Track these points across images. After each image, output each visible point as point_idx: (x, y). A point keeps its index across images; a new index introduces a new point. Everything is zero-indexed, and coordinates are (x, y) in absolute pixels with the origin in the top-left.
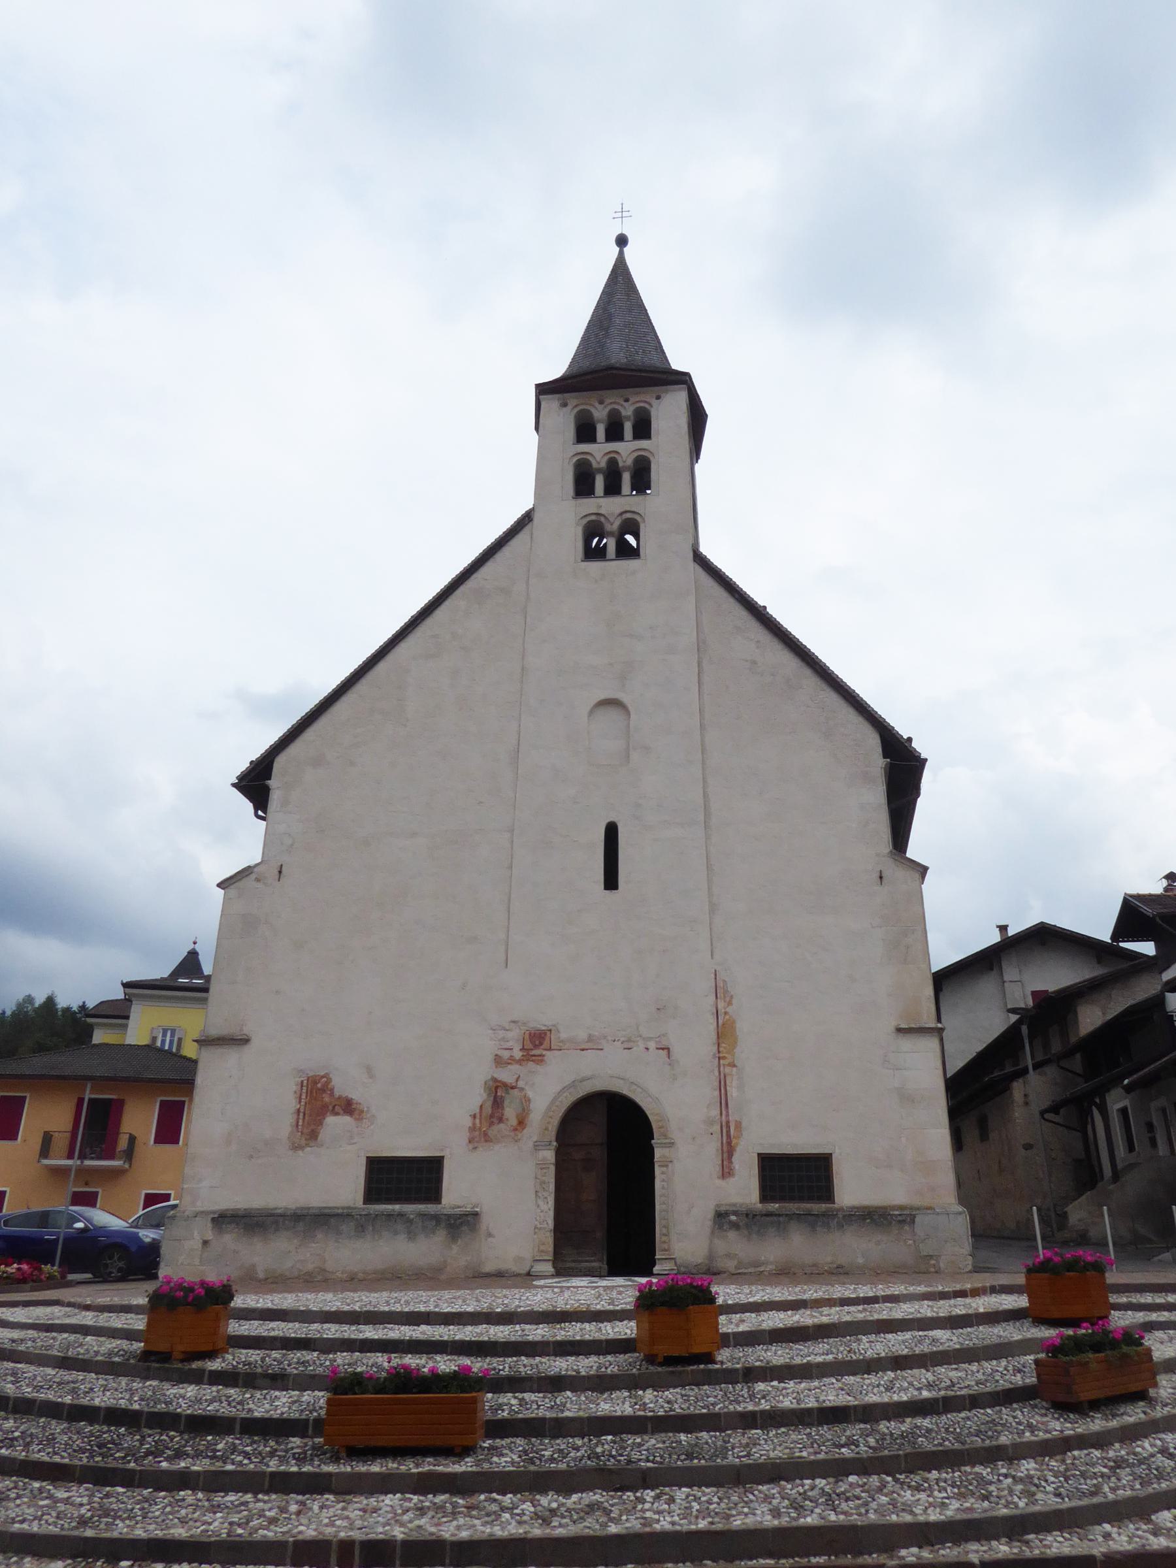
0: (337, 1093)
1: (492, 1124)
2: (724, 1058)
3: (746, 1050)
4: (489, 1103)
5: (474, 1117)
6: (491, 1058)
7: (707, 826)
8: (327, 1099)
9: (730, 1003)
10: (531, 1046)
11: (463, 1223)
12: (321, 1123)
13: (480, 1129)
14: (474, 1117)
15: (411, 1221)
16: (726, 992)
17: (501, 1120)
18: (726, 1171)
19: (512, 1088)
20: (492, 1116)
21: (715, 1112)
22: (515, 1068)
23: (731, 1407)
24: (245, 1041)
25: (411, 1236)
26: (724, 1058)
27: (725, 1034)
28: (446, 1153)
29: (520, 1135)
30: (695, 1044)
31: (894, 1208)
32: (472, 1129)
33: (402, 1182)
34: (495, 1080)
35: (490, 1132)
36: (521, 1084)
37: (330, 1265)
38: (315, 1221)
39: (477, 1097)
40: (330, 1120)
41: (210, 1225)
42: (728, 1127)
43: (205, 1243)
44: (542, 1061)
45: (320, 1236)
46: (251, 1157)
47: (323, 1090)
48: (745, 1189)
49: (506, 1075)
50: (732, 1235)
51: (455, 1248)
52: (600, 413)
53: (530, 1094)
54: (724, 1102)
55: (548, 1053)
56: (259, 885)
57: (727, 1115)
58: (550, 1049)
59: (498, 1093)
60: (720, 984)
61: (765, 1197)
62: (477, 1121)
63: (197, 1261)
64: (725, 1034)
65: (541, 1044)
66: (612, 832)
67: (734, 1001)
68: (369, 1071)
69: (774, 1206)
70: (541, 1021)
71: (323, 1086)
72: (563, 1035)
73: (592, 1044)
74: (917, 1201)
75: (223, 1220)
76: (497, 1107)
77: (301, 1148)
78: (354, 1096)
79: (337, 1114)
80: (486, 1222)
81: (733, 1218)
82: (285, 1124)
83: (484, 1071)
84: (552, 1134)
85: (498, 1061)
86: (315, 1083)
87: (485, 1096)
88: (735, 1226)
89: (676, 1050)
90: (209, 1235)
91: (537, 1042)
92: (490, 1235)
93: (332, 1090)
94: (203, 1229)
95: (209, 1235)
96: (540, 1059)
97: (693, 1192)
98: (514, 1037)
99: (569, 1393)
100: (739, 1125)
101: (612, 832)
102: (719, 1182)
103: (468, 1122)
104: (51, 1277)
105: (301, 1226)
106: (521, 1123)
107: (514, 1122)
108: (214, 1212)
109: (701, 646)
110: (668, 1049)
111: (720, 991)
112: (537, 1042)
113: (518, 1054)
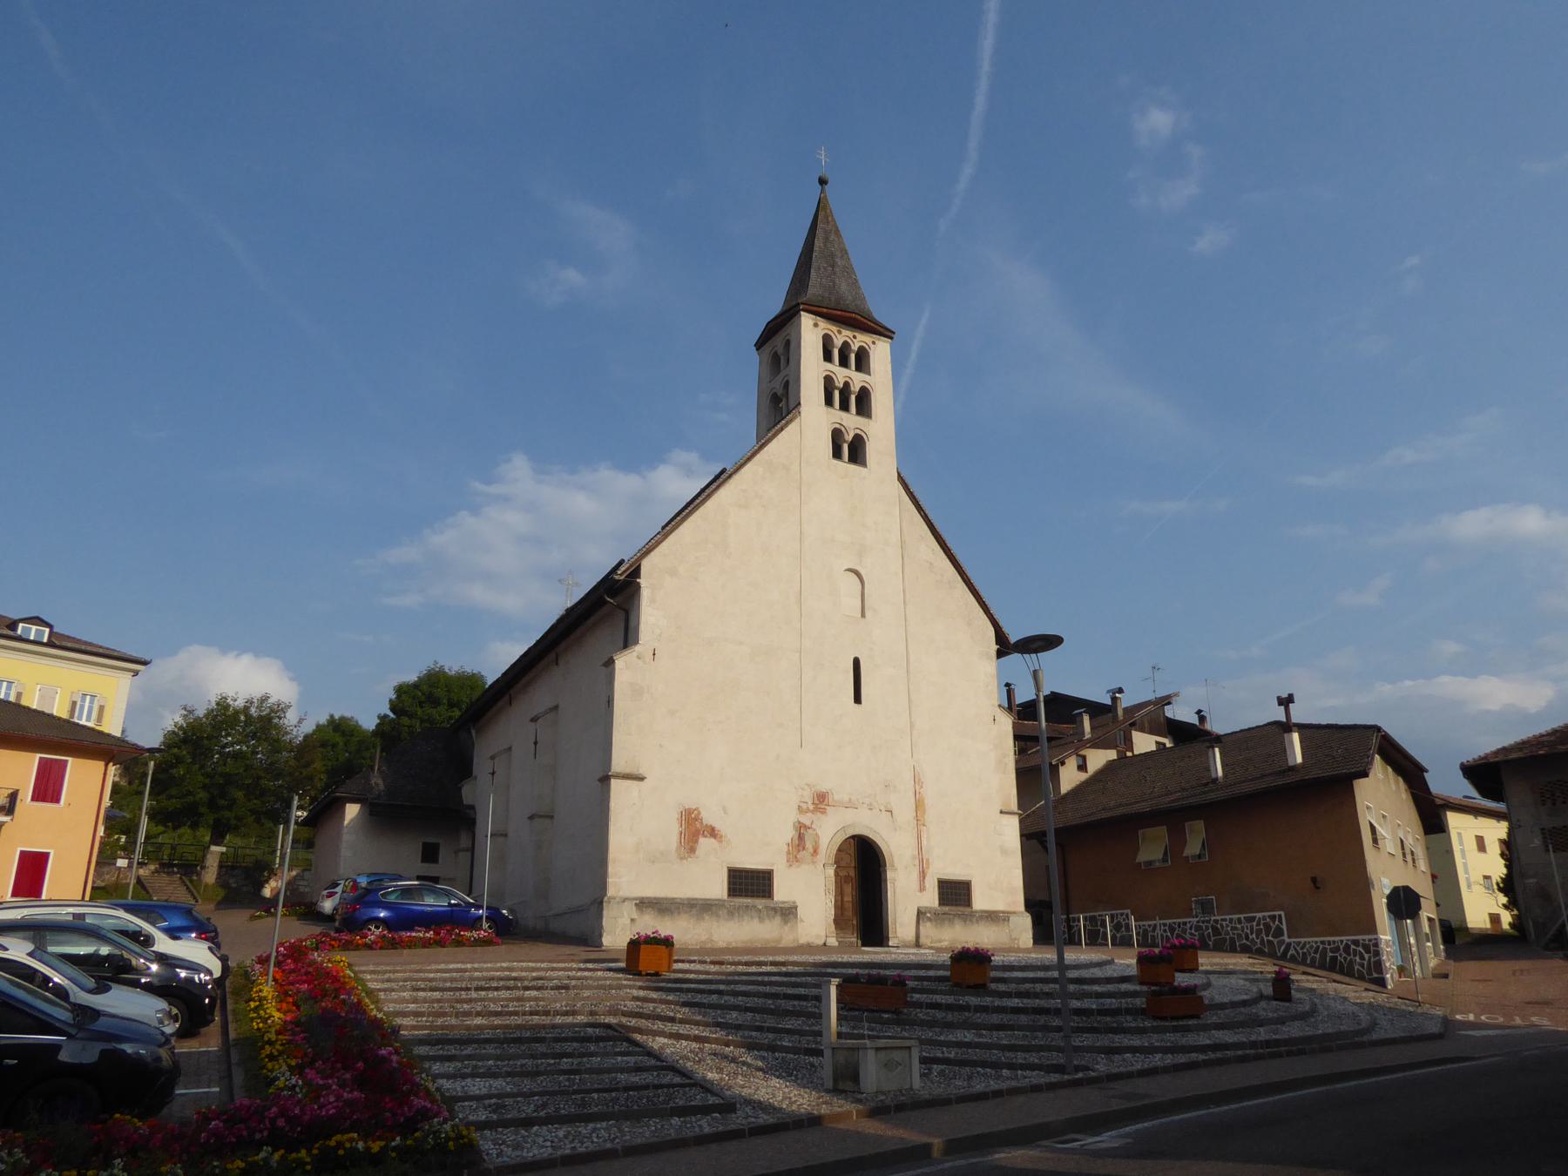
3: (930, 816)
11: (788, 913)
18: (922, 889)
24: (641, 779)
25: (761, 920)
27: (919, 805)
30: (905, 813)
33: (750, 885)
37: (715, 938)
38: (701, 908)
39: (789, 834)
40: (702, 840)
43: (633, 920)
47: (696, 819)
48: (931, 899)
49: (806, 820)
52: (838, 341)
54: (920, 849)
59: (801, 831)
64: (919, 805)
66: (856, 663)
69: (946, 909)
70: (823, 788)
73: (851, 805)
75: (644, 904)
76: (801, 840)
78: (717, 825)
82: (673, 839)
83: (793, 816)
84: (832, 860)
88: (930, 919)
94: (629, 911)
95: (635, 916)
96: (824, 812)
97: (907, 898)
98: (808, 796)
101: (856, 663)
103: (785, 848)
106: (815, 852)
111: (917, 780)
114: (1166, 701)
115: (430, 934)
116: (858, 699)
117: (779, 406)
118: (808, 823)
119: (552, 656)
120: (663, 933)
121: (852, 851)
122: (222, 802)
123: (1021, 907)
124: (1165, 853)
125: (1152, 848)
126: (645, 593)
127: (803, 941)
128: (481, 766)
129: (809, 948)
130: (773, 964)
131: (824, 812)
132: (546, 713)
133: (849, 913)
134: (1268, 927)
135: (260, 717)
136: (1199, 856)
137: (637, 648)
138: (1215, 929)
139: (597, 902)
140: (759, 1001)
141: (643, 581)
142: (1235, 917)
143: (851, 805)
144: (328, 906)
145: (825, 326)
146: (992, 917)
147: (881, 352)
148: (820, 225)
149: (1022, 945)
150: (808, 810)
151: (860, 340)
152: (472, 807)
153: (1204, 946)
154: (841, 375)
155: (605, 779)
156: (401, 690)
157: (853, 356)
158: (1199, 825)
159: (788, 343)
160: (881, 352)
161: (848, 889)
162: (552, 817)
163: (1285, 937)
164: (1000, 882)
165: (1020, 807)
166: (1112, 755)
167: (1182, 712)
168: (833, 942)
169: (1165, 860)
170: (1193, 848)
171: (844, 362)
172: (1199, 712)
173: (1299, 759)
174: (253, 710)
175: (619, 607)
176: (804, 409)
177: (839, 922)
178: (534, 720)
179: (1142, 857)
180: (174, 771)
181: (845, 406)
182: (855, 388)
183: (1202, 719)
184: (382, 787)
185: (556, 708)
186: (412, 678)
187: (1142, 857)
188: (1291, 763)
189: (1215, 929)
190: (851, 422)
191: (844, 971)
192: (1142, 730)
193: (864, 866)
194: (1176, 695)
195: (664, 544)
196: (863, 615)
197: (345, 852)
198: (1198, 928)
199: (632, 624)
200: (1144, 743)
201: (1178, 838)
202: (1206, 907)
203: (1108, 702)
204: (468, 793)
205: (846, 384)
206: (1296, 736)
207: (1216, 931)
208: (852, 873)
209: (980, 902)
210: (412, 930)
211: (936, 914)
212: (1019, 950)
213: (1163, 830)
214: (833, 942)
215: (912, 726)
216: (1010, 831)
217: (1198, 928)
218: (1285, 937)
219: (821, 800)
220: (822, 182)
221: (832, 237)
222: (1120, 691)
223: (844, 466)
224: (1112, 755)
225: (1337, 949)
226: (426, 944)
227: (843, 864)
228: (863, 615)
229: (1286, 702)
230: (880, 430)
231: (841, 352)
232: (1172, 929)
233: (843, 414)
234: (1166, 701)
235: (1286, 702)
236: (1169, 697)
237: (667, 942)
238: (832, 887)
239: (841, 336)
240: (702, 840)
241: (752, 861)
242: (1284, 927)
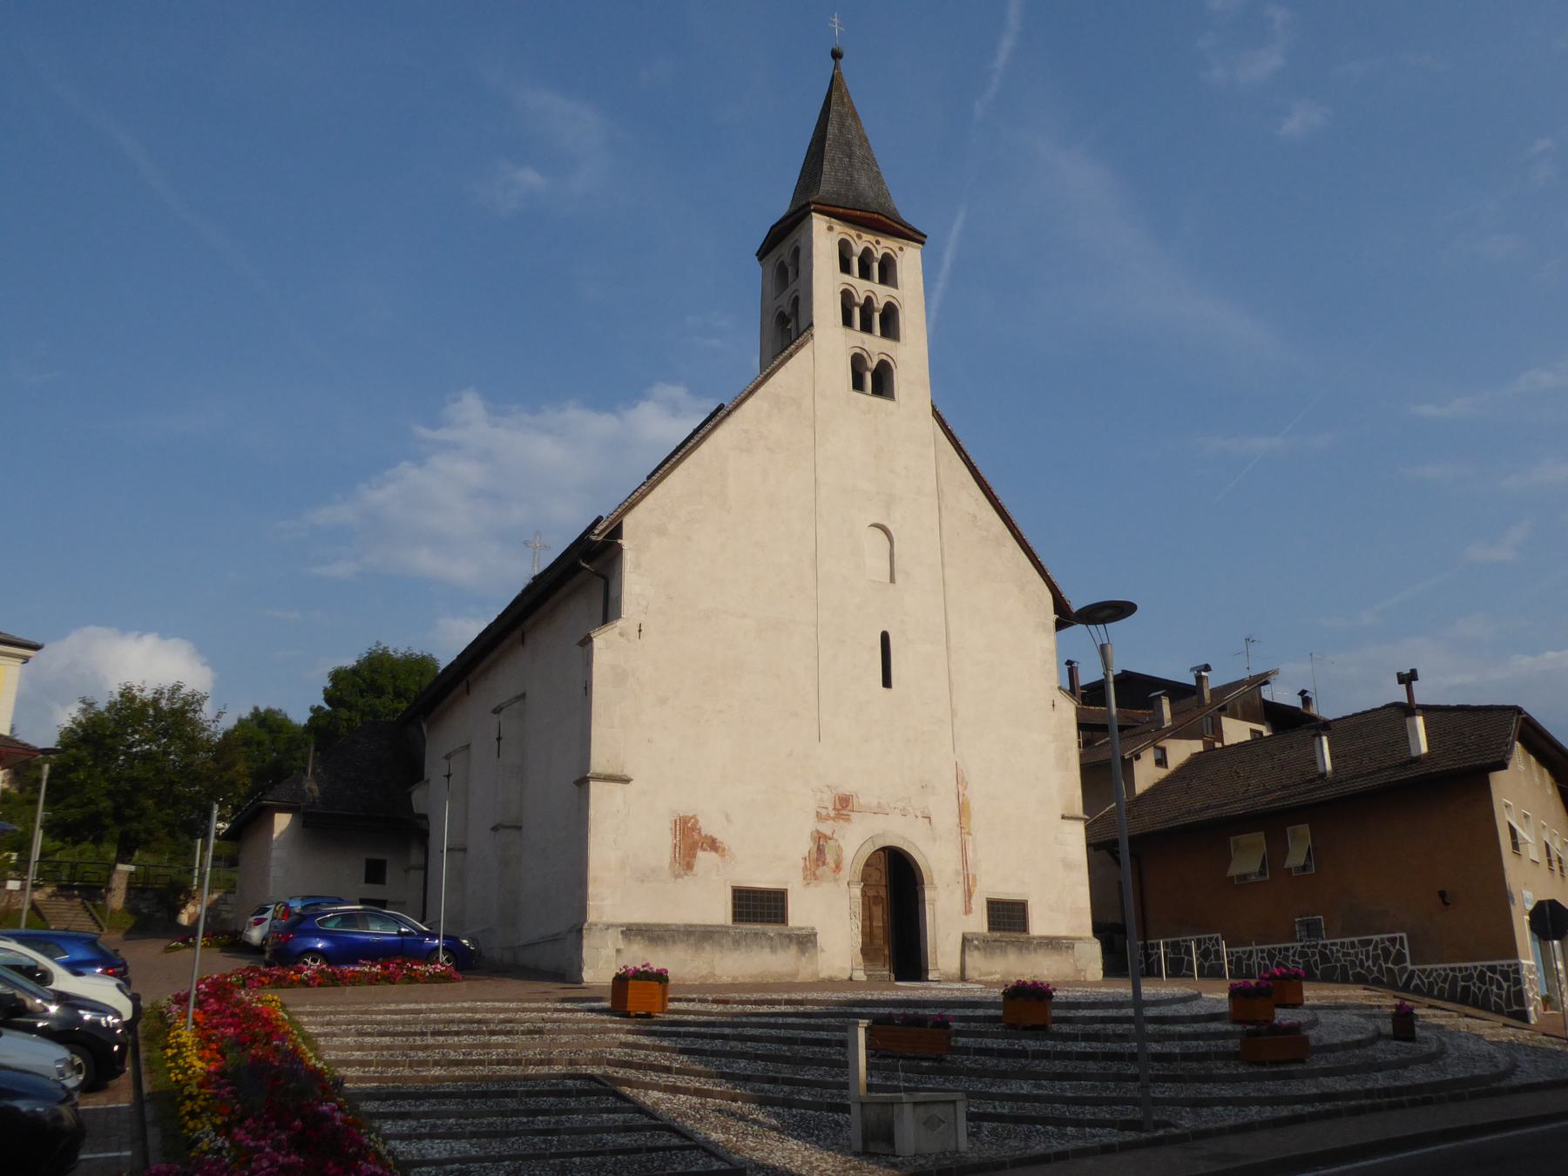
3: (977, 822)
11: (806, 941)
12: (694, 856)
15: (771, 939)
24: (626, 781)
25: (773, 949)
27: (963, 810)
28: (789, 887)
30: (947, 818)
32: (805, 869)
33: (759, 907)
37: (718, 972)
39: (805, 846)
40: (700, 854)
43: (618, 951)
48: (978, 922)
49: (826, 828)
50: (976, 954)
52: (858, 248)
54: (965, 862)
56: (622, 640)
61: (990, 929)
64: (963, 810)
66: (885, 638)
68: (727, 817)
70: (846, 789)
73: (879, 810)
75: (632, 932)
76: (820, 854)
77: (677, 877)
78: (719, 837)
80: (821, 940)
83: (809, 825)
84: (858, 877)
88: (977, 948)
94: (614, 940)
96: (847, 819)
97: (949, 922)
98: (828, 801)
101: (885, 638)
103: (802, 863)
105: (692, 940)
106: (838, 867)
111: (960, 779)
113: (832, 814)
114: (1263, 680)
115: (377, 969)
116: (887, 682)
117: (787, 328)
118: (829, 833)
119: (517, 633)
120: (656, 965)
121: (882, 866)
122: (128, 812)
123: (1087, 930)
124: (1263, 865)
125: (1246, 859)
126: (628, 557)
127: (824, 974)
128: (434, 768)
129: (831, 983)
130: (789, 1002)
131: (847, 819)
132: (510, 703)
133: (879, 941)
134: (1386, 952)
135: (173, 712)
136: (1304, 868)
137: (619, 623)
138: (1323, 956)
139: (577, 930)
140: (772, 1047)
141: (626, 542)
142: (1347, 940)
143: (879, 810)
144: (256, 935)
145: (841, 230)
146: (1053, 944)
147: (909, 260)
148: (834, 107)
149: (1090, 978)
150: (828, 818)
151: (885, 246)
152: (425, 817)
153: (1310, 976)
154: (862, 288)
155: (583, 782)
156: (338, 677)
157: (876, 266)
158: (1304, 830)
159: (797, 252)
160: (909, 260)
161: (878, 912)
162: (519, 828)
163: (1408, 964)
164: (1062, 899)
165: (1085, 811)
166: (1197, 746)
167: (1282, 693)
168: (860, 975)
169: (1262, 873)
170: (1296, 857)
171: (865, 273)
172: (1303, 693)
173: (1424, 749)
174: (163, 703)
175: (597, 574)
176: (817, 331)
177: (868, 952)
178: (497, 711)
179: (1234, 870)
180: (72, 776)
181: (866, 327)
182: (879, 304)
183: (1307, 701)
184: (317, 794)
185: (523, 696)
186: (349, 662)
187: (1234, 870)
188: (1414, 754)
189: (1323, 956)
190: (875, 346)
191: (874, 1010)
192: (1234, 716)
193: (897, 885)
194: (1275, 672)
195: (650, 497)
196: (892, 580)
197: (275, 872)
198: (1303, 955)
199: (612, 594)
200: (1236, 731)
201: (1277, 847)
202: (1312, 929)
203: (1193, 682)
204: (419, 799)
205: (869, 300)
206: (1420, 721)
207: (1325, 958)
208: (883, 893)
209: (1039, 926)
210: (356, 963)
211: (985, 941)
212: (1086, 984)
213: (1260, 837)
214: (860, 975)
215: (954, 713)
216: (1076, 836)
217: (1303, 955)
218: (1408, 964)
219: (844, 805)
220: (836, 55)
221: (849, 121)
222: (1207, 668)
223: (866, 400)
224: (1197, 746)
225: (1470, 977)
226: (373, 980)
227: (871, 881)
228: (892, 580)
229: (1408, 679)
230: (910, 355)
231: (861, 260)
232: (1271, 956)
233: (865, 336)
234: (1263, 680)
235: (1408, 679)
236: (1266, 674)
237: (661, 977)
238: (859, 910)
239: (861, 242)
240: (700, 854)
241: (761, 879)
242: (1407, 951)
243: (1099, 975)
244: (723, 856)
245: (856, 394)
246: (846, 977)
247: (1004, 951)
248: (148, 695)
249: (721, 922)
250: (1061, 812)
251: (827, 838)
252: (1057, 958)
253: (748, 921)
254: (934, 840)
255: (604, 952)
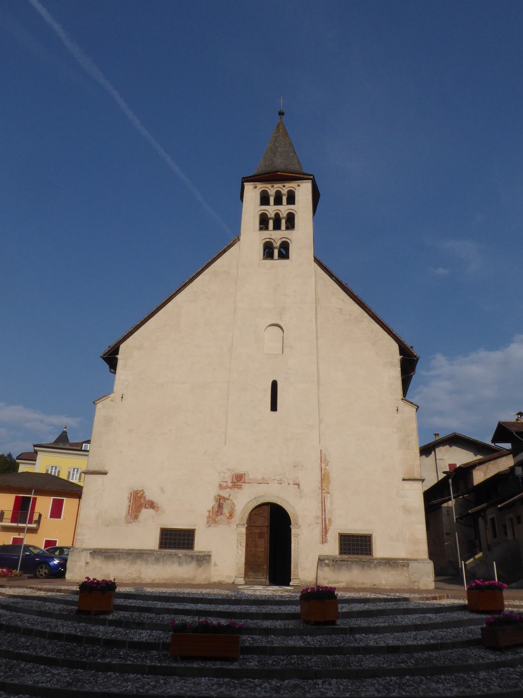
0: (147, 499)
1: (218, 515)
2: (324, 489)
3: (334, 486)
4: (217, 506)
5: (210, 511)
6: (218, 485)
7: (318, 384)
8: (142, 501)
9: (327, 465)
10: (236, 481)
11: (204, 559)
12: (140, 511)
13: (212, 517)
14: (210, 511)
15: (180, 557)
16: (326, 459)
17: (221, 514)
18: (324, 540)
19: (227, 499)
20: (218, 512)
21: (320, 514)
22: (228, 490)
23: (348, 645)
24: (106, 474)
25: (180, 564)
26: (324, 489)
27: (325, 478)
28: (196, 528)
29: (230, 521)
31: (399, 559)
32: (209, 517)
33: (177, 540)
34: (219, 496)
35: (216, 519)
36: (231, 498)
37: (143, 576)
38: (137, 555)
39: (211, 504)
41: (89, 555)
42: (325, 520)
44: (241, 488)
45: (139, 562)
46: (108, 525)
48: (332, 548)
49: (224, 493)
50: (326, 569)
51: (200, 570)
53: (236, 503)
54: (324, 510)
55: (243, 484)
57: (325, 515)
58: (245, 483)
59: (220, 503)
60: (323, 456)
61: (341, 553)
62: (211, 514)
63: (83, 571)
64: (325, 478)
65: (241, 480)
66: (274, 385)
67: (329, 464)
68: (162, 490)
69: (346, 557)
70: (240, 470)
71: (141, 495)
72: (251, 477)
73: (264, 481)
74: (410, 557)
75: (96, 553)
76: (220, 509)
77: (130, 523)
78: (155, 500)
79: (146, 508)
80: (213, 559)
81: (327, 561)
84: (245, 521)
85: (221, 487)
86: (137, 494)
87: (215, 503)
88: (327, 565)
89: (302, 485)
90: (89, 560)
91: (239, 480)
92: (216, 565)
93: (145, 497)
94: (86, 557)
96: (240, 487)
98: (228, 478)
99: (273, 636)
100: (330, 520)
101: (274, 385)
102: (321, 545)
103: (207, 514)
104: (16, 575)
105: (130, 558)
106: (231, 516)
107: (228, 515)
108: (91, 550)
109: (317, 301)
110: (299, 484)
111: (323, 459)
112: (239, 480)
113: (230, 485)
116: (274, 407)
118: (226, 496)
143: (264, 481)
146: (390, 563)
149: (422, 587)
150: (227, 487)
151: (285, 188)
154: (271, 210)
164: (402, 533)
176: (243, 237)
209: (380, 551)
220: (281, 114)
223: (277, 263)
239: (272, 190)
240: (144, 510)
243: (431, 585)
244: (158, 511)
245: (269, 262)
246: (231, 582)
247: (349, 568)
248: (6, 455)
249: (153, 548)
250: (402, 477)
251: (225, 499)
252: (393, 572)
253: (170, 548)
254: (301, 497)
255: (79, 564)
